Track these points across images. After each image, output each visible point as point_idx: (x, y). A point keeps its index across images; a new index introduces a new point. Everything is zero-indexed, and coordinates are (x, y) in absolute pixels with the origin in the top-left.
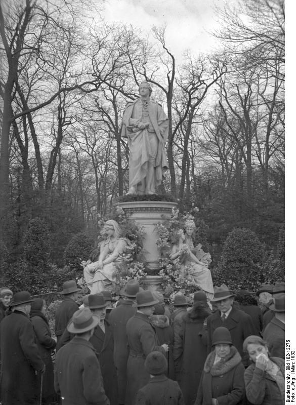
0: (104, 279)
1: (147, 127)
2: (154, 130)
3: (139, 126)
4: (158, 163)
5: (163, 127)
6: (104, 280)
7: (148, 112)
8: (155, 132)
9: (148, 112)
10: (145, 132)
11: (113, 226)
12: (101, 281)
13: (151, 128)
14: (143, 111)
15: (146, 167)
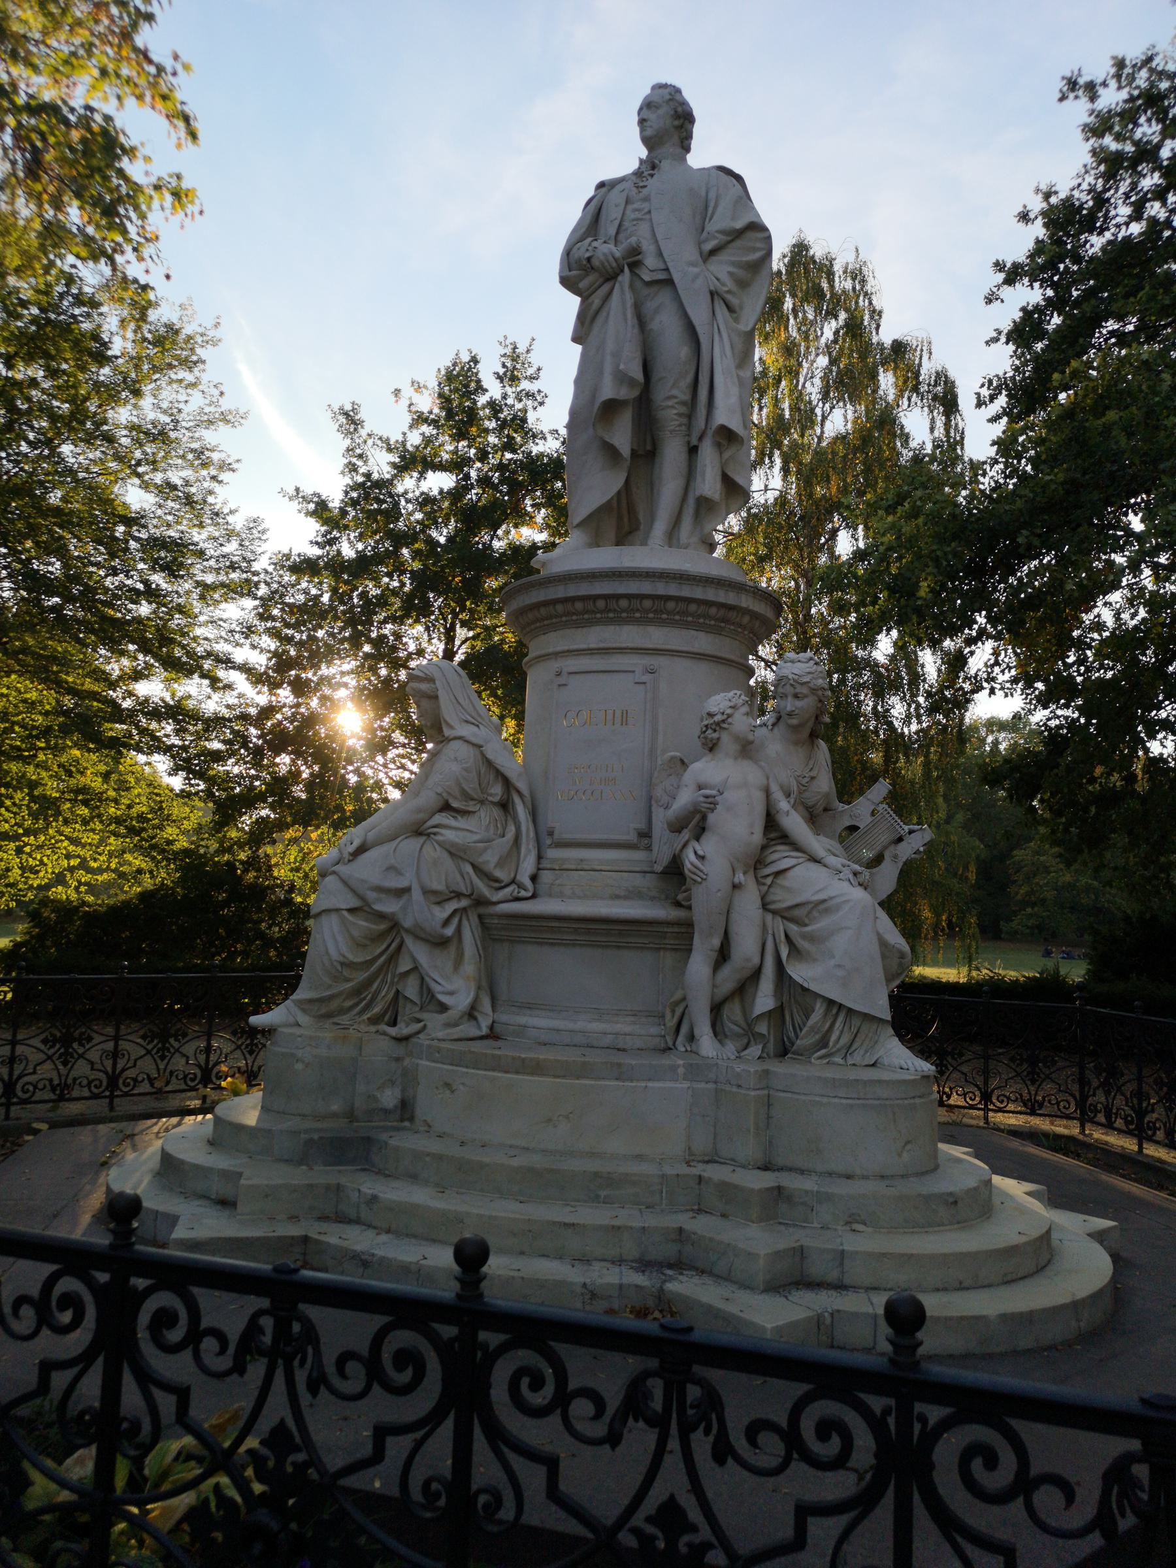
0: (354, 903)
1: (633, 260)
2: (667, 270)
3: (595, 262)
4: (700, 422)
5: (733, 264)
6: (350, 910)
7: (647, 199)
8: (669, 282)
9: (647, 199)
10: (626, 276)
11: (430, 680)
12: (337, 910)
13: (650, 261)
14: (628, 201)
15: (622, 437)
